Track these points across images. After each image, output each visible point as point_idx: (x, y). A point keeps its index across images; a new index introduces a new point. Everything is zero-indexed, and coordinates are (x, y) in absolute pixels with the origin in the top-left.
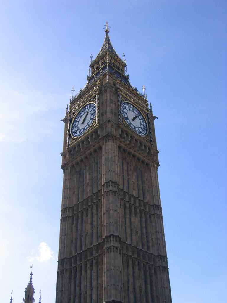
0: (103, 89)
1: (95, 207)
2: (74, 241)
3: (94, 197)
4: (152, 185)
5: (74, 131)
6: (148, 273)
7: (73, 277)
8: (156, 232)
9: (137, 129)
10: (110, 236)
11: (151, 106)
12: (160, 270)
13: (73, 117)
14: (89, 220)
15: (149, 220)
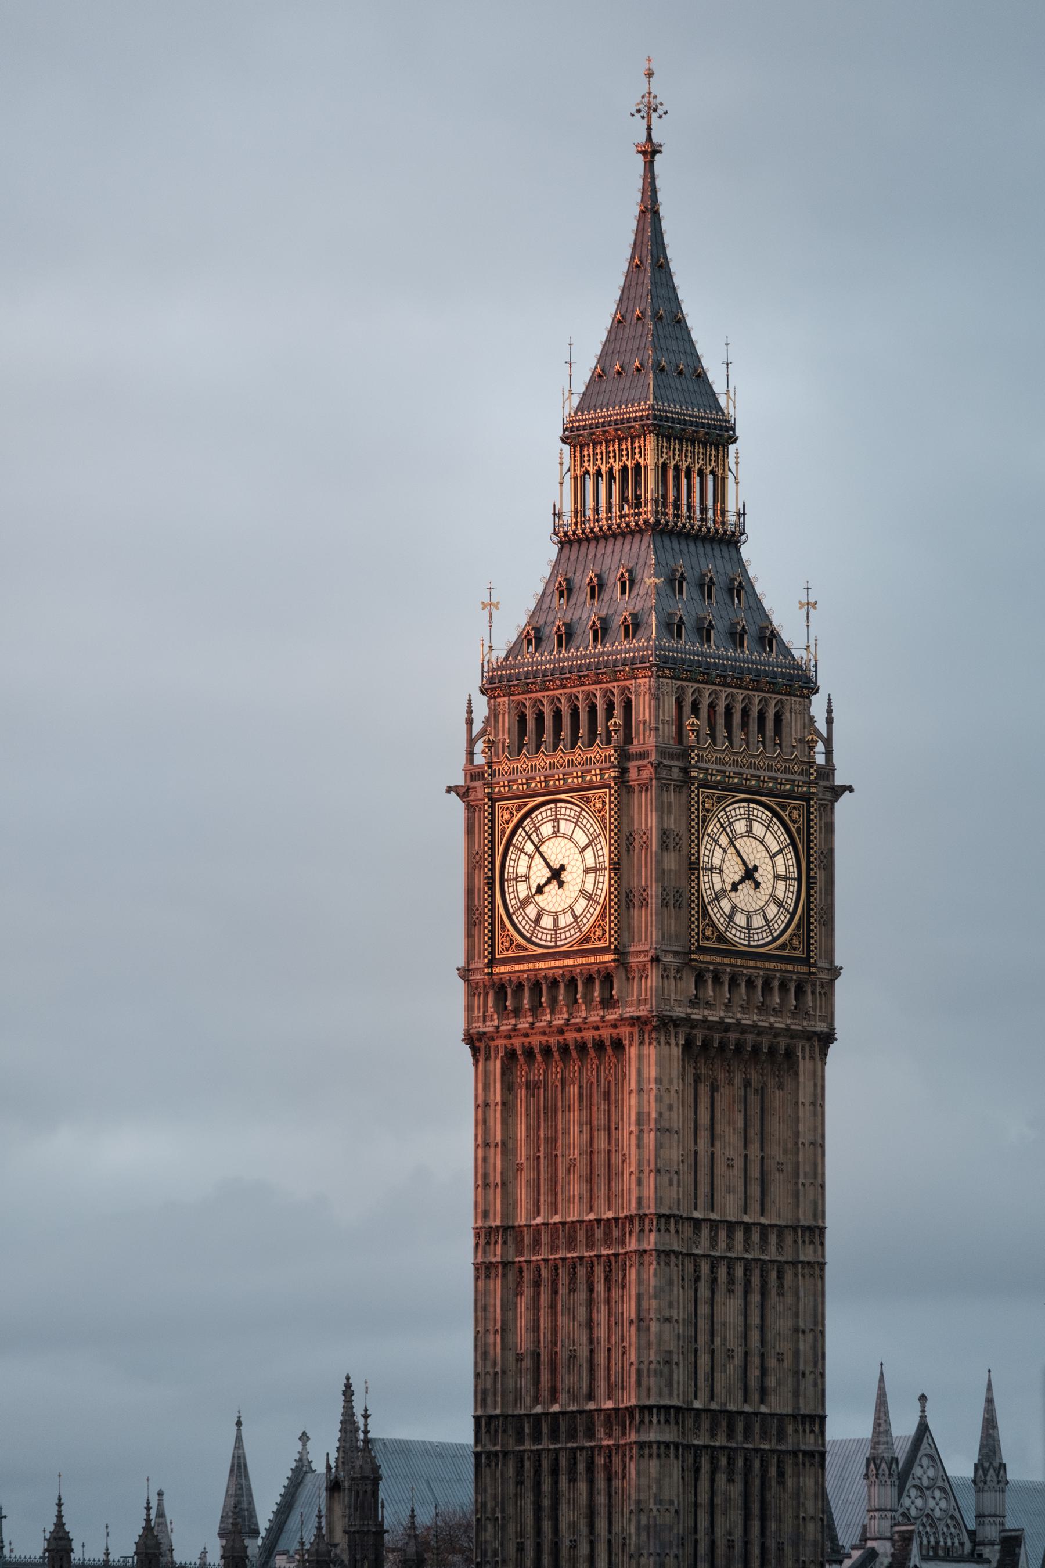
0: (633, 774)
1: (599, 1272)
2: (527, 1363)
3: (599, 1234)
4: (796, 1144)
5: (512, 903)
6: (757, 1482)
7: (528, 1483)
8: (796, 1330)
9: (757, 921)
10: (650, 1408)
11: (829, 721)
12: (797, 1464)
13: (506, 816)
14: (581, 1313)
15: (773, 1292)
